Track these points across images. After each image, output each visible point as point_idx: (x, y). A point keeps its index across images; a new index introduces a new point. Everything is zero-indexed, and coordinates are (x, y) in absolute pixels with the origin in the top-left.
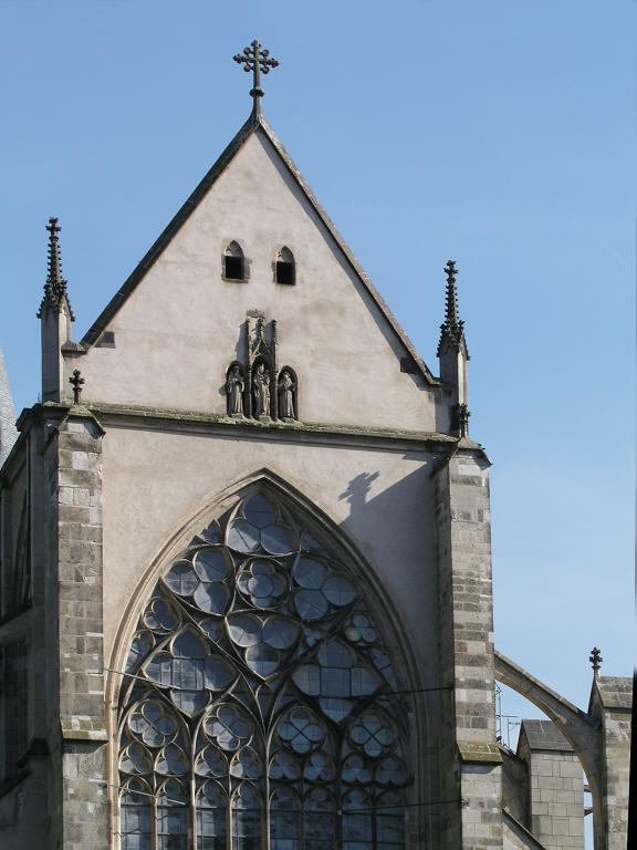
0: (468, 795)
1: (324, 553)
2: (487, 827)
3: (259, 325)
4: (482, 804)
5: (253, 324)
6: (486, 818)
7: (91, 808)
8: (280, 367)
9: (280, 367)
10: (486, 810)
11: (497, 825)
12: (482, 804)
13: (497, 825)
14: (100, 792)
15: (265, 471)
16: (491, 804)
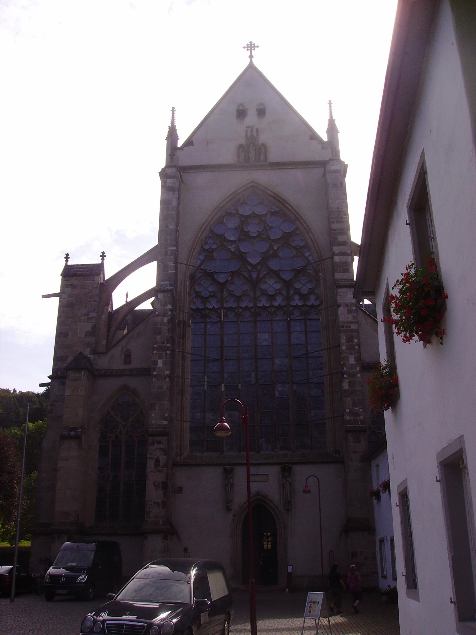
0: (340, 302)
1: (281, 212)
2: (350, 316)
3: (252, 131)
4: (347, 306)
5: (249, 130)
6: (349, 312)
7: (166, 319)
8: (260, 144)
9: (260, 144)
10: (349, 308)
11: (355, 315)
12: (347, 306)
13: (355, 315)
14: (170, 313)
15: (252, 182)
16: (352, 304)
